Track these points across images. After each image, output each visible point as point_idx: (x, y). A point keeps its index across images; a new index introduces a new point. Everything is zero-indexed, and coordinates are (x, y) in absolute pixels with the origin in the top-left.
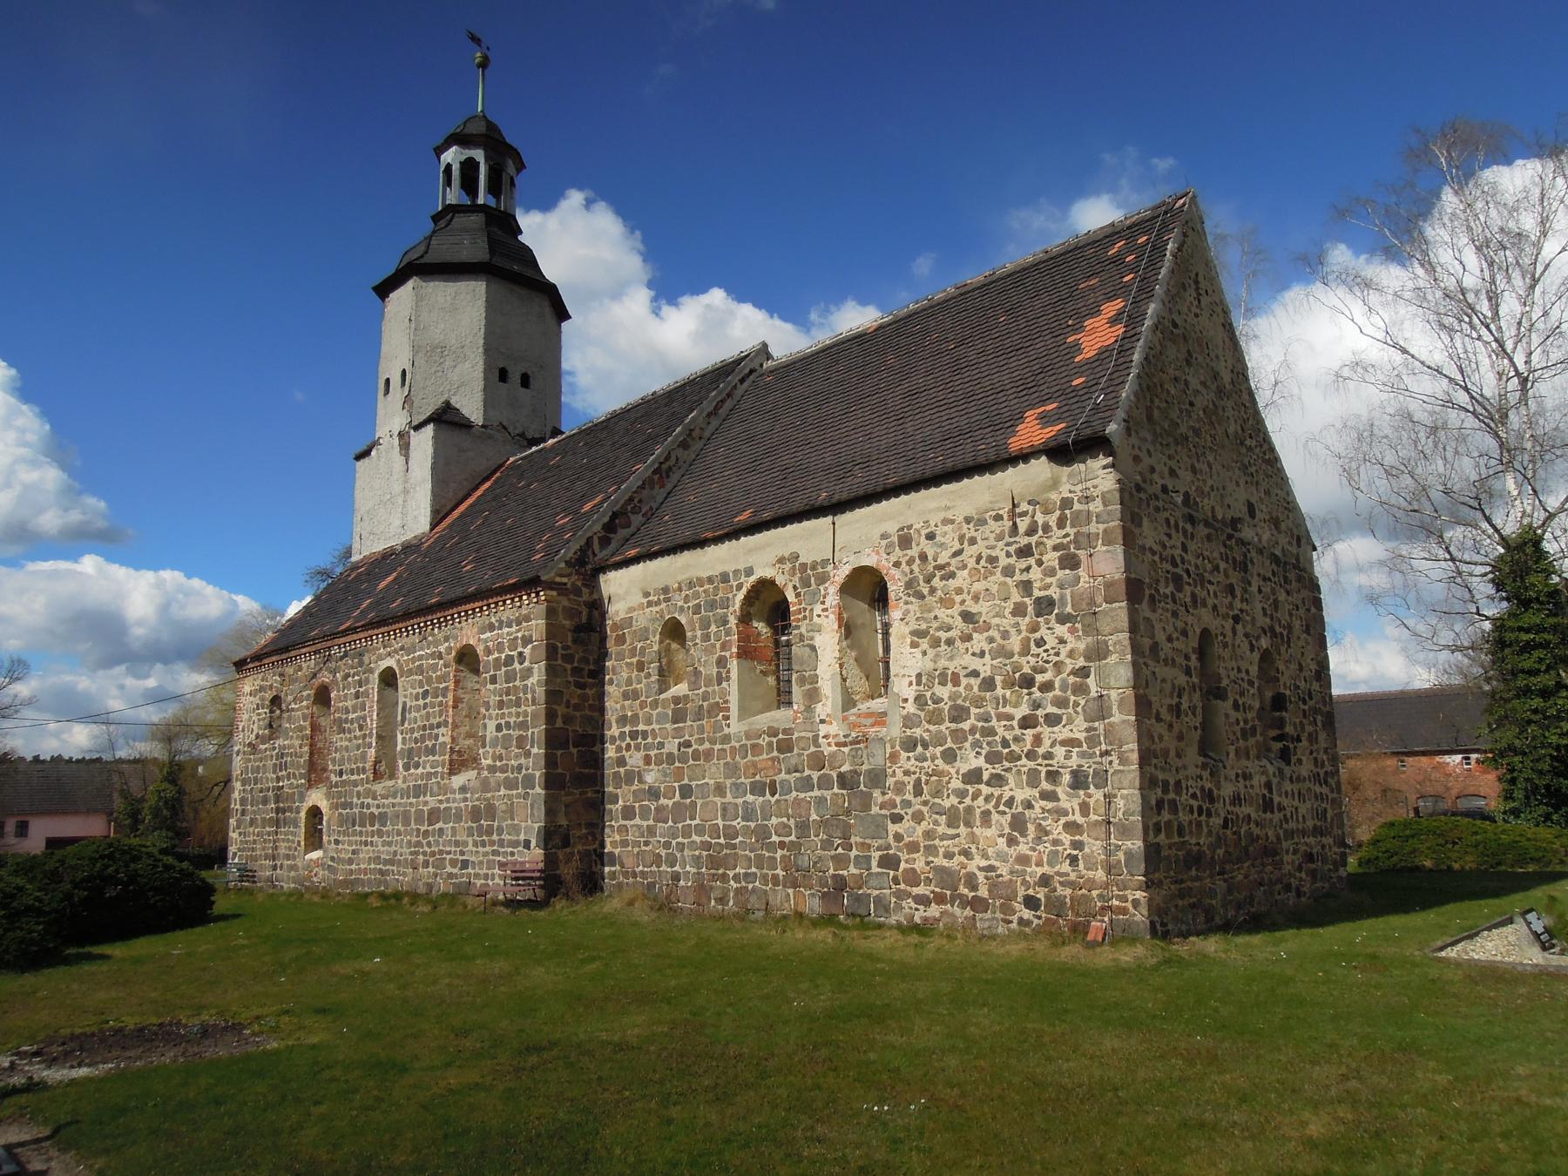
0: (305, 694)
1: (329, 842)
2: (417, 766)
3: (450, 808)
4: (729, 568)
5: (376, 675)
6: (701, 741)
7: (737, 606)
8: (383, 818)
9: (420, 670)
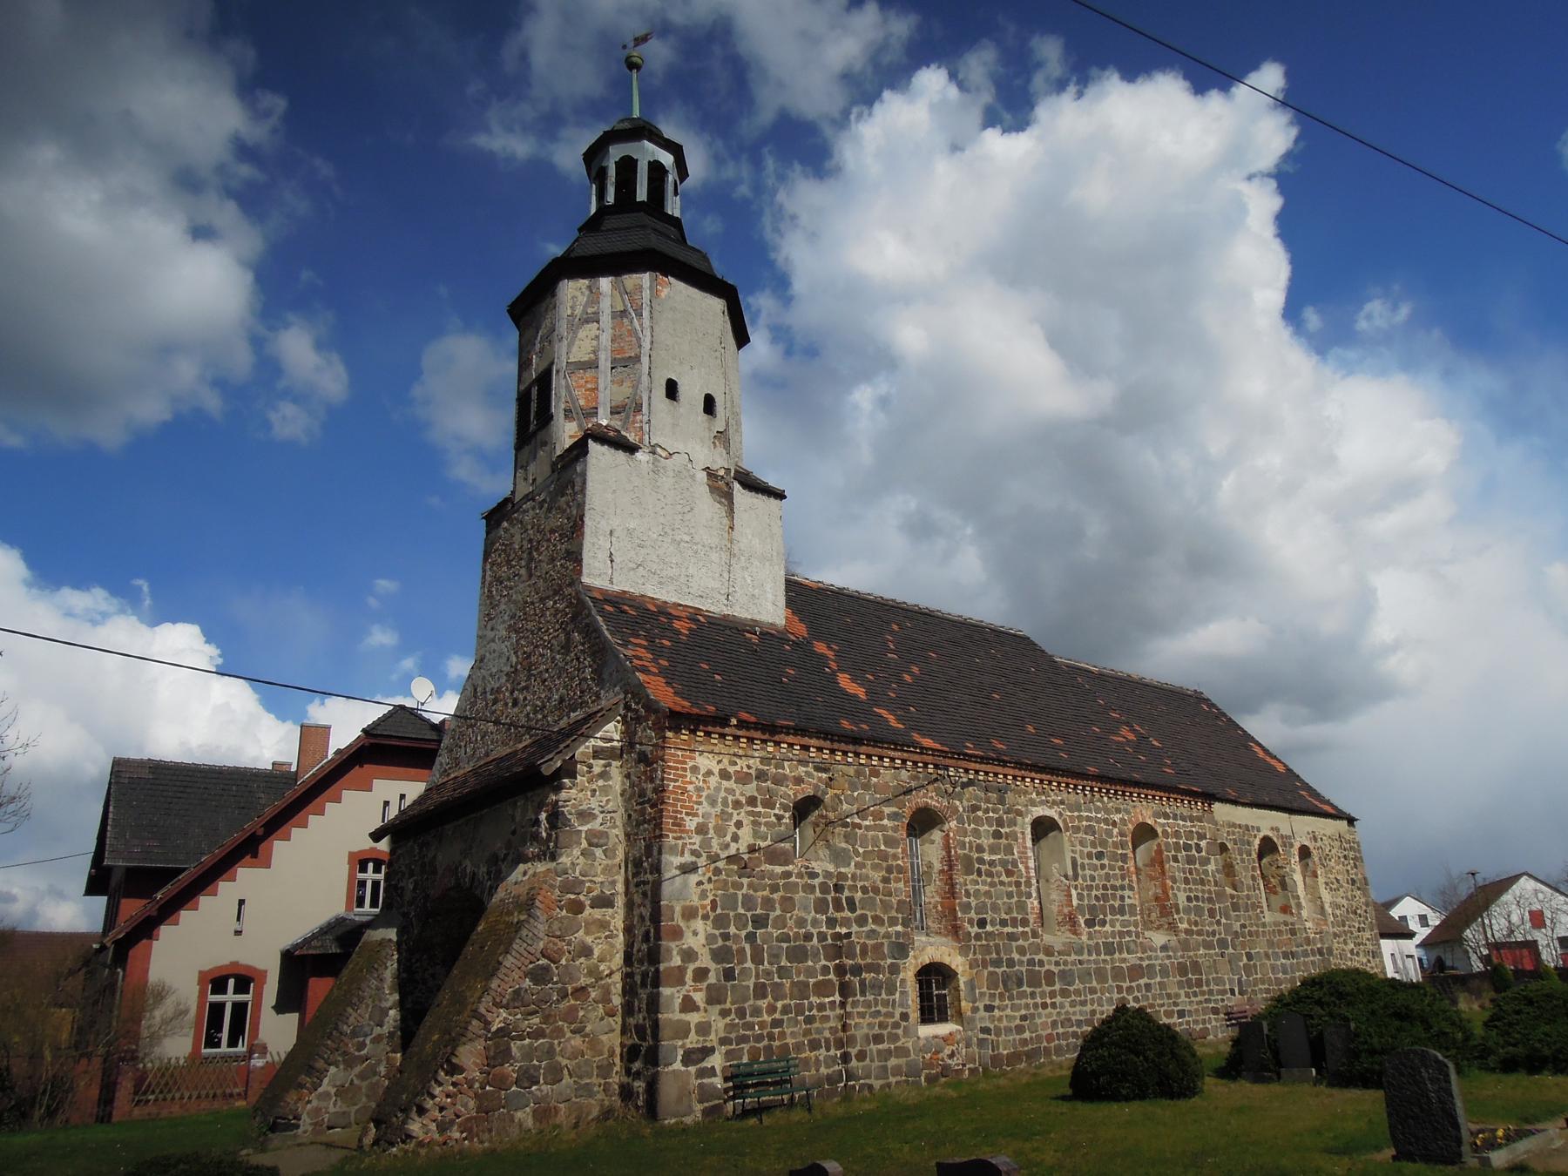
0: (887, 810)
1: (975, 1010)
2: (1103, 923)
3: (1154, 965)
4: (1250, 824)
5: (1029, 819)
6: (1251, 925)
7: (1257, 847)
8: (1066, 977)
9: (1090, 830)
